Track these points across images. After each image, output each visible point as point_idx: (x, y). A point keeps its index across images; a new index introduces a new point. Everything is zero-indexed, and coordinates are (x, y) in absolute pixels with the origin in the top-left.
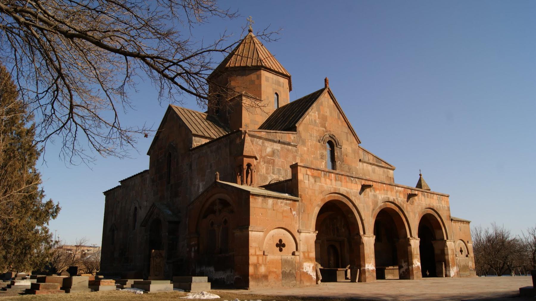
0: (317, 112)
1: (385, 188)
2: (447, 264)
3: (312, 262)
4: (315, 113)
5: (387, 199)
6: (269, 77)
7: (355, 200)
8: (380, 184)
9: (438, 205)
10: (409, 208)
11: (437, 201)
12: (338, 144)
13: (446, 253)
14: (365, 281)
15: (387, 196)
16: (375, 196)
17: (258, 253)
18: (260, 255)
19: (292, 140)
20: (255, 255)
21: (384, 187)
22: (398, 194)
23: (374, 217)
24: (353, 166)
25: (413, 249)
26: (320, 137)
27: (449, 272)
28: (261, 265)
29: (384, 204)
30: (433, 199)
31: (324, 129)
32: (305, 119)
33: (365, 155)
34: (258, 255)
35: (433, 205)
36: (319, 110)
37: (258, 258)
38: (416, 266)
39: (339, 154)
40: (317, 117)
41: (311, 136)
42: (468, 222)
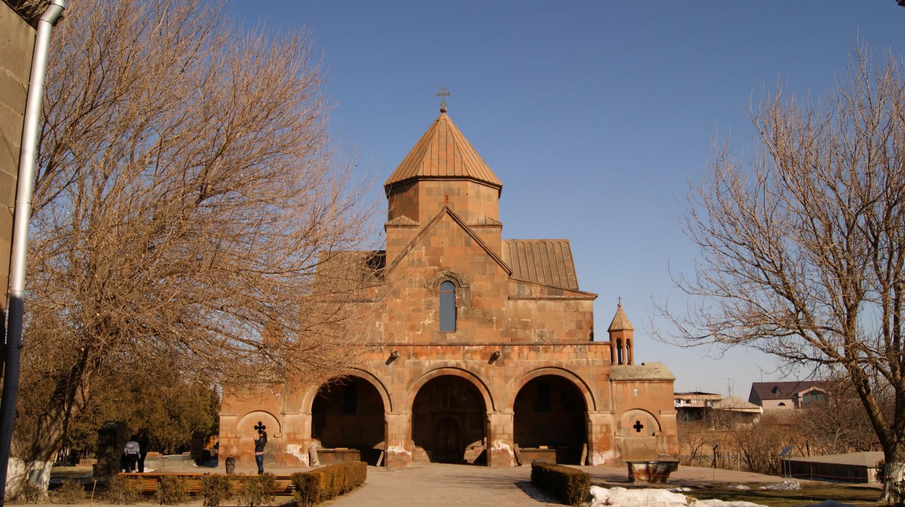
0: (424, 248)
1: (441, 351)
2: (590, 447)
3: (299, 444)
4: (421, 249)
5: (442, 364)
6: (431, 188)
7: (377, 373)
8: (429, 347)
9: (573, 360)
10: (491, 372)
11: (573, 355)
12: (461, 283)
13: (589, 430)
14: (387, 466)
15: (443, 361)
16: (419, 363)
17: (229, 435)
18: (232, 438)
19: (376, 294)
20: (226, 437)
21: (438, 350)
22: (469, 355)
23: (414, 389)
24: (493, 308)
25: (495, 427)
26: (427, 280)
27: (592, 458)
28: (232, 447)
29: (438, 372)
30: (562, 352)
31: (436, 267)
32: (402, 261)
33: (524, 288)
34: (228, 438)
35: (560, 362)
36: (428, 245)
37: (229, 441)
38: (497, 448)
39: (464, 296)
40: (424, 254)
41: (410, 282)
42: (670, 381)
